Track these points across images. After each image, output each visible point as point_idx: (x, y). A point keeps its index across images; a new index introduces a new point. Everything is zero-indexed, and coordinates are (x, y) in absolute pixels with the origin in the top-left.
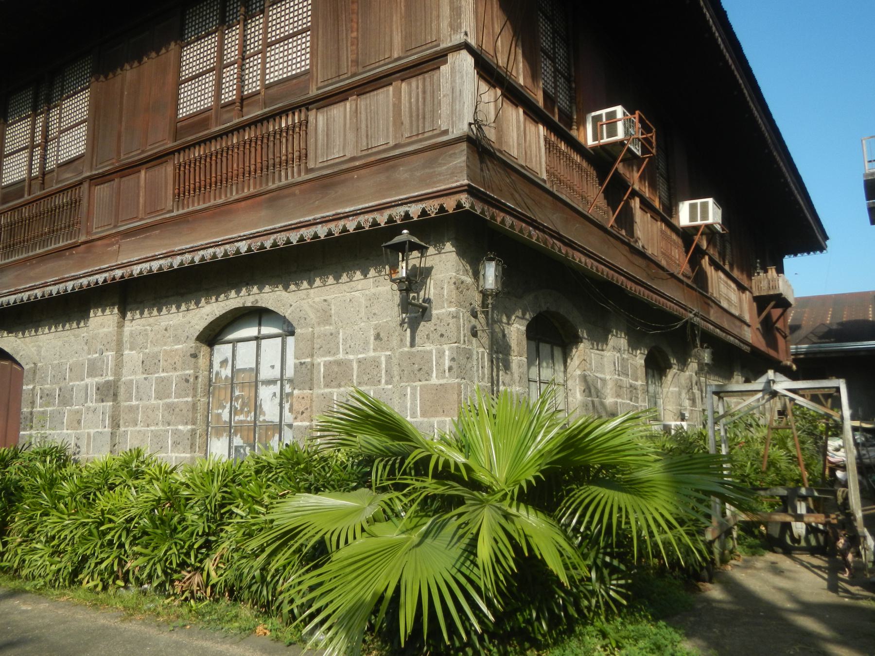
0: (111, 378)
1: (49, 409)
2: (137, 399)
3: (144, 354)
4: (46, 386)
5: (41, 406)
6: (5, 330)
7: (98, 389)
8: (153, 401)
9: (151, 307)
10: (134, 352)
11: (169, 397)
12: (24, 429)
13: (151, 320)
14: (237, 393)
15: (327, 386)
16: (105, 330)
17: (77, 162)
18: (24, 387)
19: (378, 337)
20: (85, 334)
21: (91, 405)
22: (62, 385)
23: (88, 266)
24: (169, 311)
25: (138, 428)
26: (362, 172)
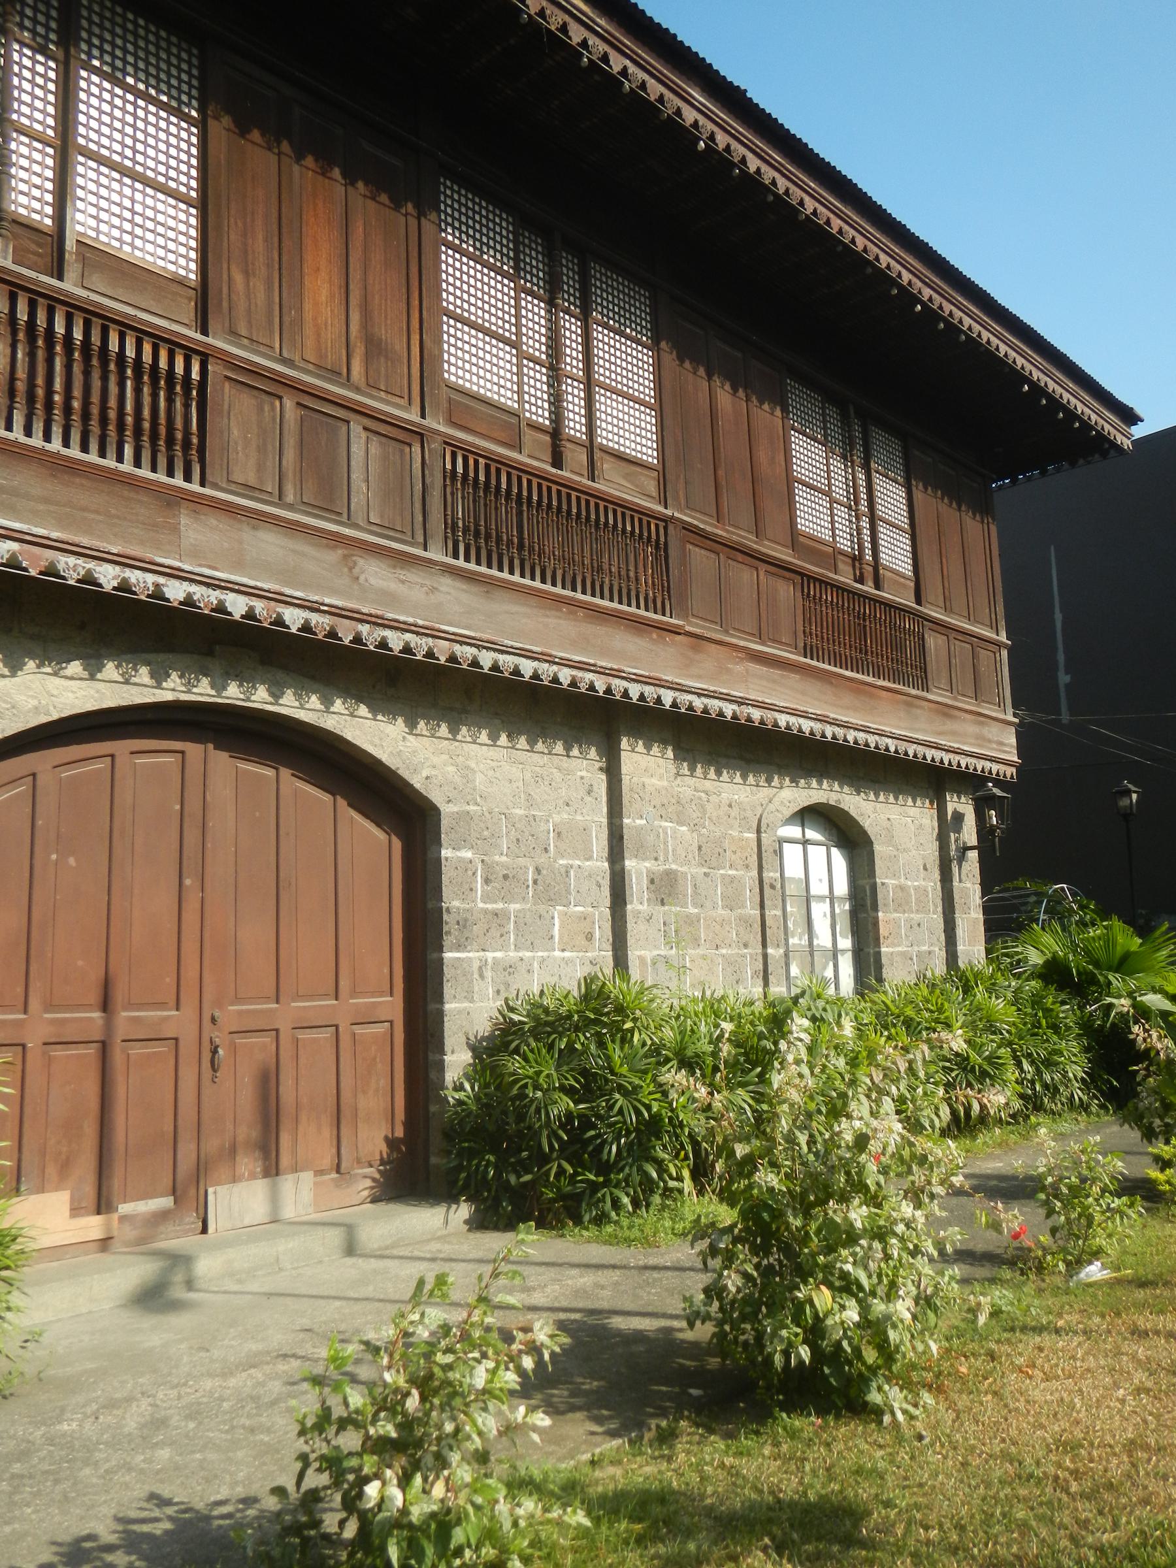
0: (674, 867)
1: (514, 907)
2: (695, 905)
3: (700, 835)
4: (497, 858)
5: (486, 898)
6: (360, 699)
7: (652, 881)
8: (720, 911)
9: (708, 763)
10: (684, 828)
11: (743, 906)
12: (459, 947)
13: (707, 783)
14: (789, 909)
15: (895, 911)
16: (654, 781)
17: (639, 469)
18: (443, 852)
19: (925, 869)
20: (584, 773)
21: (640, 907)
22: (542, 860)
23: (699, 677)
24: (705, 774)
25: (700, 951)
26: (968, 716)
